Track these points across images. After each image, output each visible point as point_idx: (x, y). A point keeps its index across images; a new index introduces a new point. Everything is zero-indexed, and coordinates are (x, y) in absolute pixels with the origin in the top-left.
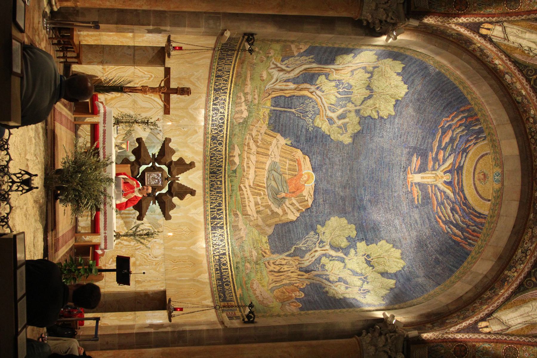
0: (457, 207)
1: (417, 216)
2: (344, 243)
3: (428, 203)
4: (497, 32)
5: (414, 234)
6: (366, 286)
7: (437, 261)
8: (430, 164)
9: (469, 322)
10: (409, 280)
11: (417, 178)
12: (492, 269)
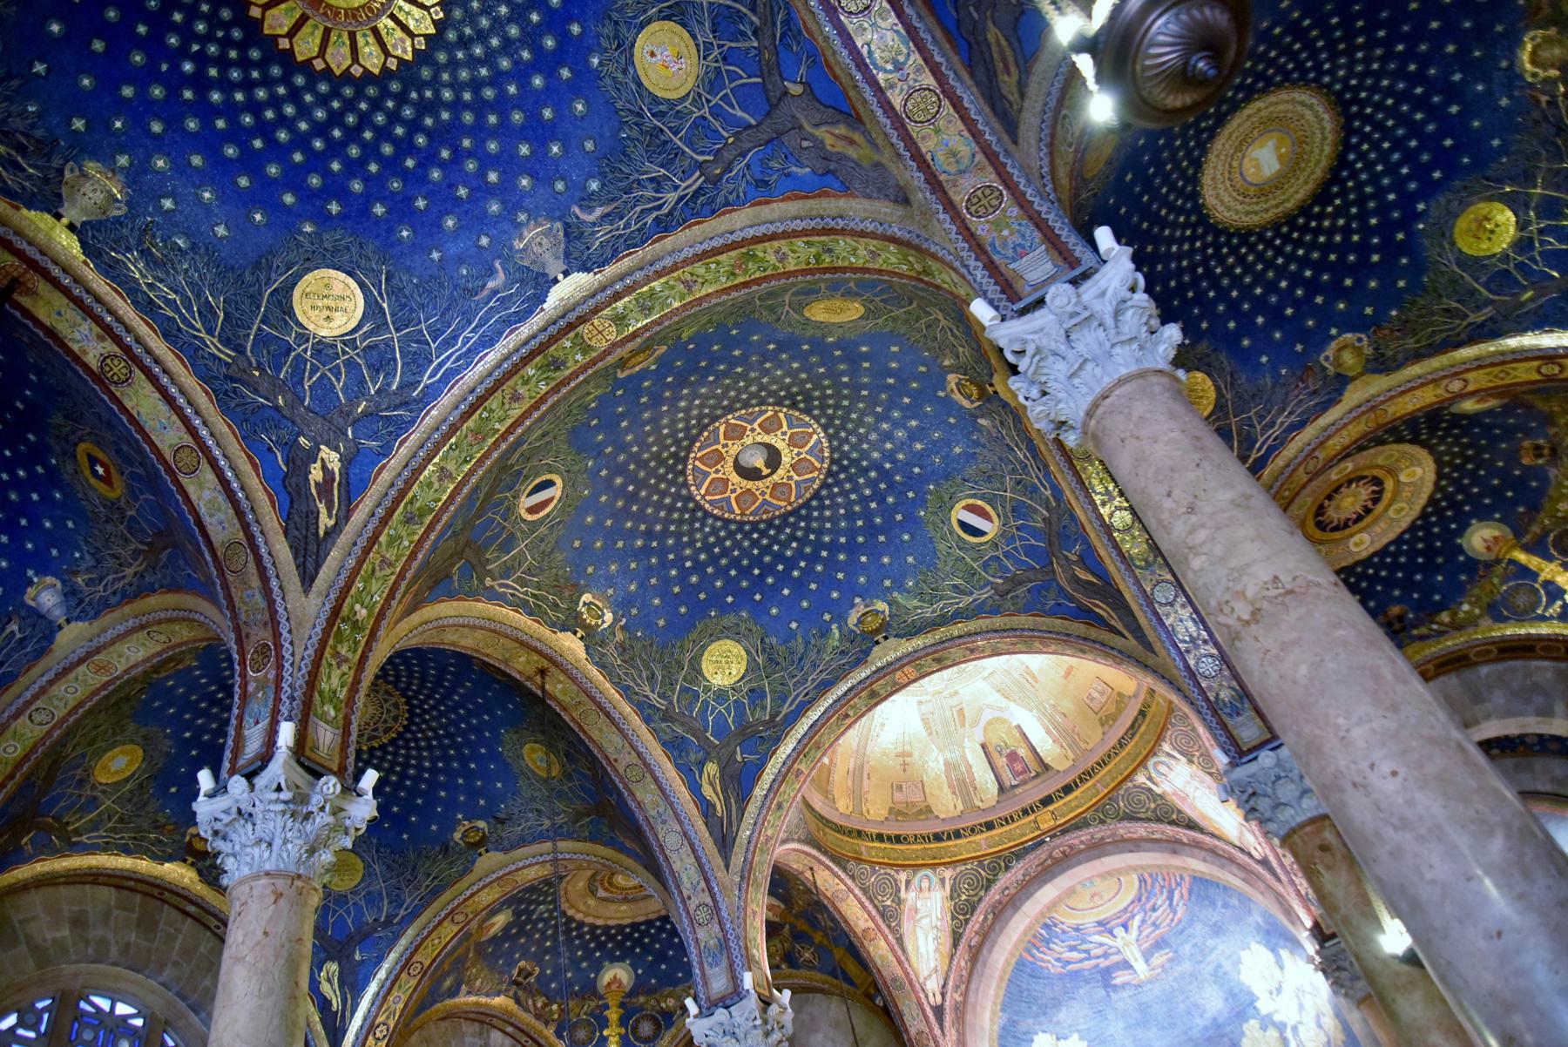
0: (1149, 906)
1: (1187, 947)
2: (1273, 1033)
3: (1163, 940)
4: (933, 985)
5: (1210, 942)
7: (1226, 905)
8: (1114, 959)
9: (1259, 869)
10: (1268, 933)
11: (1140, 966)
12: (1193, 856)
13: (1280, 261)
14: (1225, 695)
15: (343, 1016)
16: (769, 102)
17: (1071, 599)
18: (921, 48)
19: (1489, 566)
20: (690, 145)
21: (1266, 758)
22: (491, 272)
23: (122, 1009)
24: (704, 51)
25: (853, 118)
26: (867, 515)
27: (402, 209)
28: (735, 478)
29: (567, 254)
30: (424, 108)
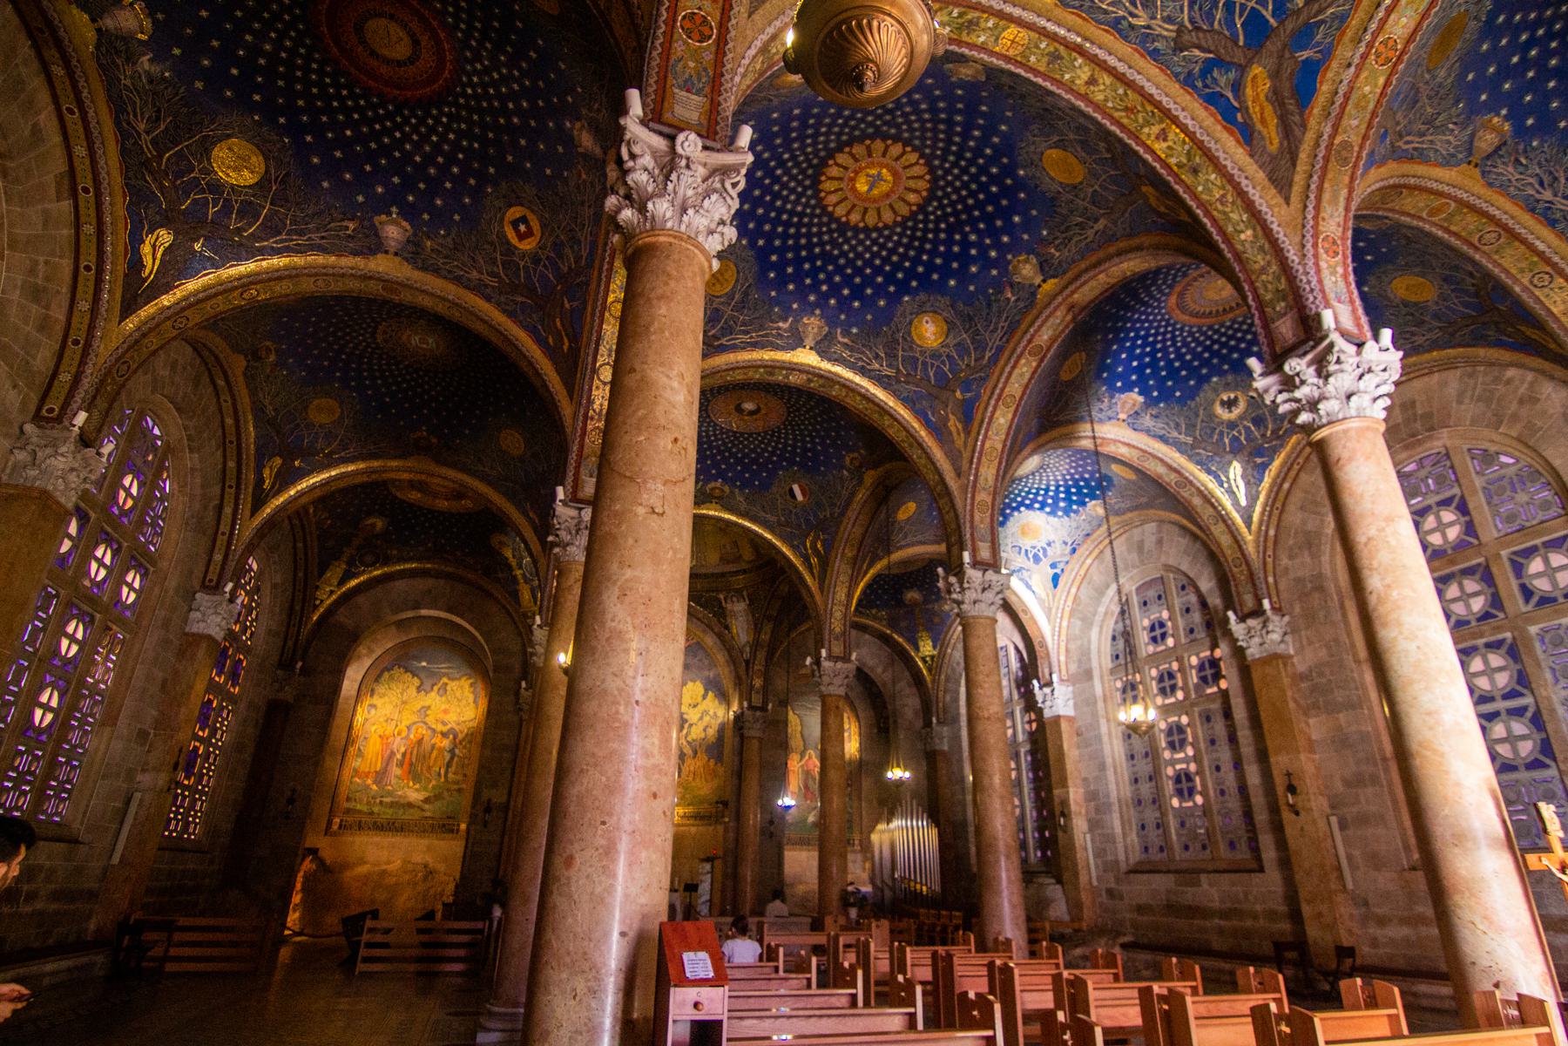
6: (711, 713)
13: (858, 280)
14: (838, 630)
15: (267, 495)
16: (944, 383)
17: (806, 549)
18: (1008, 434)
19: (906, 606)
20: (903, 360)
21: (839, 665)
22: (785, 320)
23: (157, 431)
24: (943, 345)
25: (968, 432)
26: (759, 455)
27: (780, 267)
28: (732, 407)
29: (818, 343)
30: (833, 242)
